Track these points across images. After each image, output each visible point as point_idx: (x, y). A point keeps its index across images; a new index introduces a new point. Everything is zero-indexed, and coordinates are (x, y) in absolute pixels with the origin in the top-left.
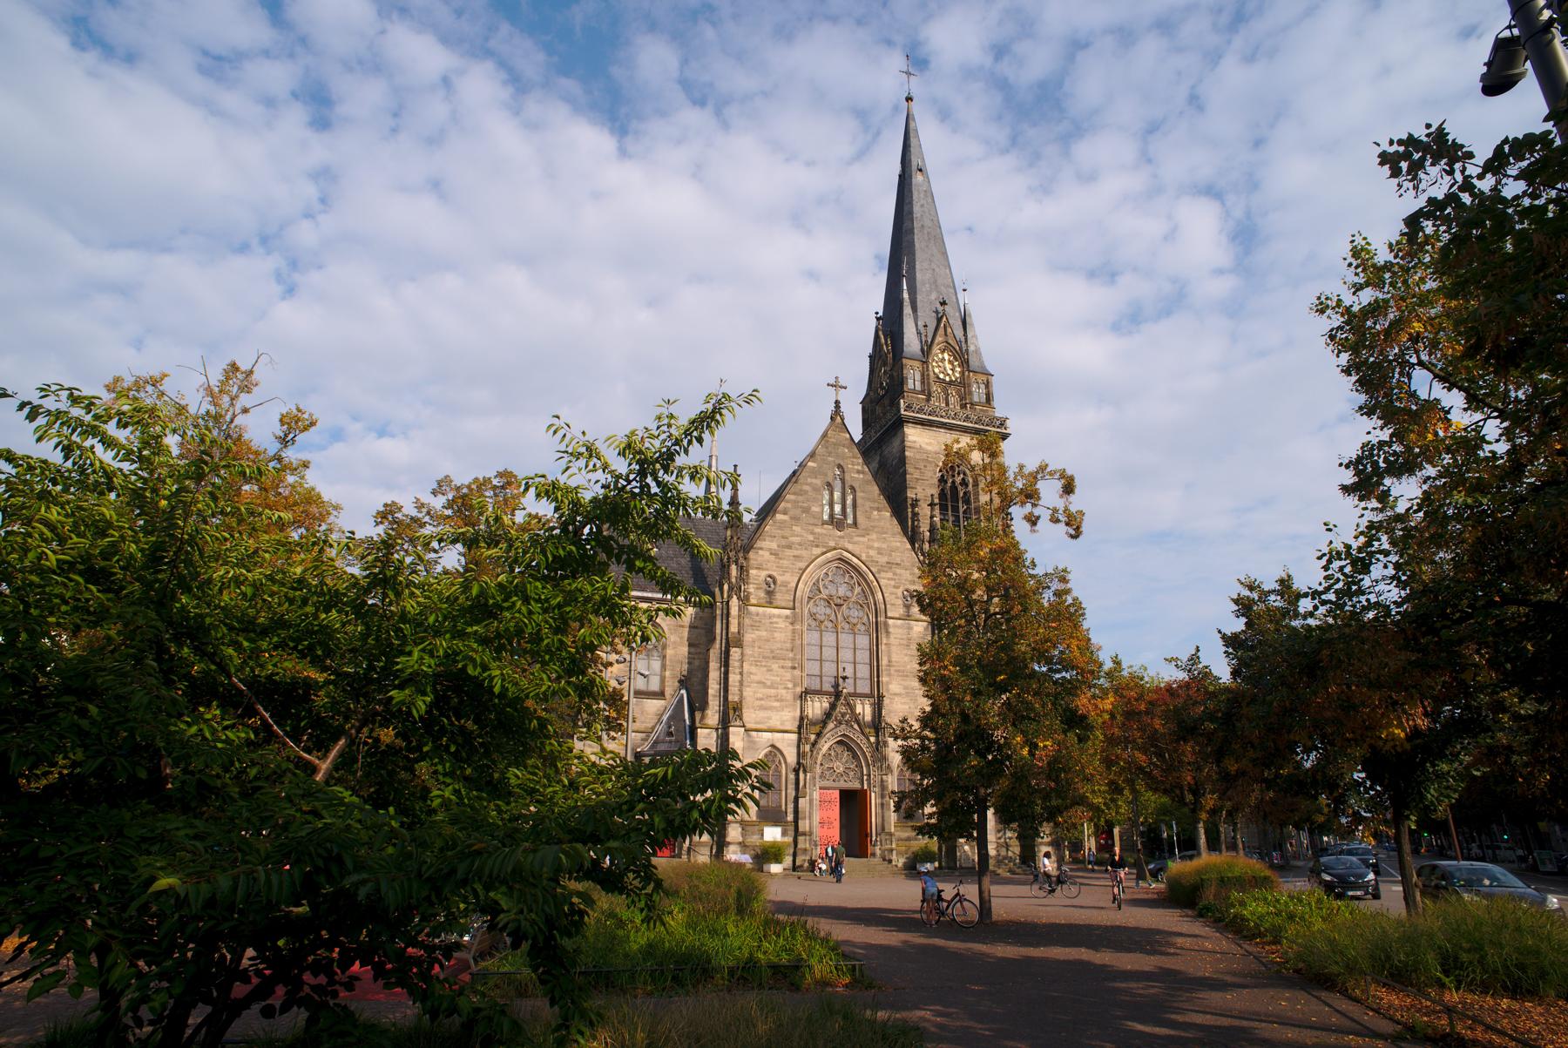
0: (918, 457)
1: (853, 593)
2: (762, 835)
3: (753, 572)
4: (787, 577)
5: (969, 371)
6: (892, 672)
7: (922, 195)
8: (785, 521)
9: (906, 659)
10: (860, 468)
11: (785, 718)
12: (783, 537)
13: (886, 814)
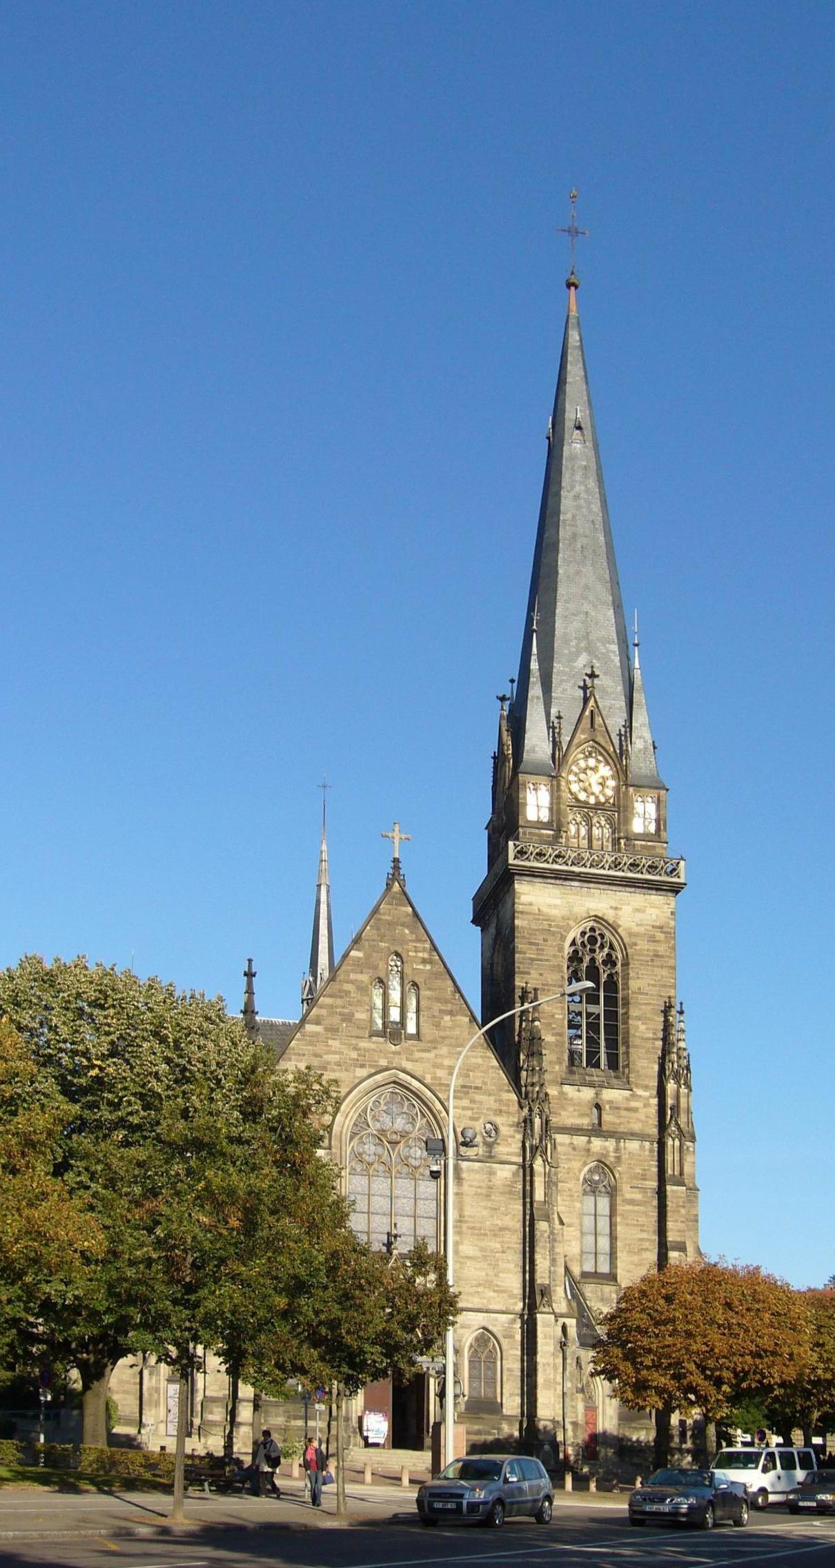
0: (533, 927)
1: (414, 1126)
5: (627, 785)
6: (464, 1229)
7: (578, 477)
8: (317, 1034)
9: (485, 1213)
10: (426, 955)
12: (316, 1055)
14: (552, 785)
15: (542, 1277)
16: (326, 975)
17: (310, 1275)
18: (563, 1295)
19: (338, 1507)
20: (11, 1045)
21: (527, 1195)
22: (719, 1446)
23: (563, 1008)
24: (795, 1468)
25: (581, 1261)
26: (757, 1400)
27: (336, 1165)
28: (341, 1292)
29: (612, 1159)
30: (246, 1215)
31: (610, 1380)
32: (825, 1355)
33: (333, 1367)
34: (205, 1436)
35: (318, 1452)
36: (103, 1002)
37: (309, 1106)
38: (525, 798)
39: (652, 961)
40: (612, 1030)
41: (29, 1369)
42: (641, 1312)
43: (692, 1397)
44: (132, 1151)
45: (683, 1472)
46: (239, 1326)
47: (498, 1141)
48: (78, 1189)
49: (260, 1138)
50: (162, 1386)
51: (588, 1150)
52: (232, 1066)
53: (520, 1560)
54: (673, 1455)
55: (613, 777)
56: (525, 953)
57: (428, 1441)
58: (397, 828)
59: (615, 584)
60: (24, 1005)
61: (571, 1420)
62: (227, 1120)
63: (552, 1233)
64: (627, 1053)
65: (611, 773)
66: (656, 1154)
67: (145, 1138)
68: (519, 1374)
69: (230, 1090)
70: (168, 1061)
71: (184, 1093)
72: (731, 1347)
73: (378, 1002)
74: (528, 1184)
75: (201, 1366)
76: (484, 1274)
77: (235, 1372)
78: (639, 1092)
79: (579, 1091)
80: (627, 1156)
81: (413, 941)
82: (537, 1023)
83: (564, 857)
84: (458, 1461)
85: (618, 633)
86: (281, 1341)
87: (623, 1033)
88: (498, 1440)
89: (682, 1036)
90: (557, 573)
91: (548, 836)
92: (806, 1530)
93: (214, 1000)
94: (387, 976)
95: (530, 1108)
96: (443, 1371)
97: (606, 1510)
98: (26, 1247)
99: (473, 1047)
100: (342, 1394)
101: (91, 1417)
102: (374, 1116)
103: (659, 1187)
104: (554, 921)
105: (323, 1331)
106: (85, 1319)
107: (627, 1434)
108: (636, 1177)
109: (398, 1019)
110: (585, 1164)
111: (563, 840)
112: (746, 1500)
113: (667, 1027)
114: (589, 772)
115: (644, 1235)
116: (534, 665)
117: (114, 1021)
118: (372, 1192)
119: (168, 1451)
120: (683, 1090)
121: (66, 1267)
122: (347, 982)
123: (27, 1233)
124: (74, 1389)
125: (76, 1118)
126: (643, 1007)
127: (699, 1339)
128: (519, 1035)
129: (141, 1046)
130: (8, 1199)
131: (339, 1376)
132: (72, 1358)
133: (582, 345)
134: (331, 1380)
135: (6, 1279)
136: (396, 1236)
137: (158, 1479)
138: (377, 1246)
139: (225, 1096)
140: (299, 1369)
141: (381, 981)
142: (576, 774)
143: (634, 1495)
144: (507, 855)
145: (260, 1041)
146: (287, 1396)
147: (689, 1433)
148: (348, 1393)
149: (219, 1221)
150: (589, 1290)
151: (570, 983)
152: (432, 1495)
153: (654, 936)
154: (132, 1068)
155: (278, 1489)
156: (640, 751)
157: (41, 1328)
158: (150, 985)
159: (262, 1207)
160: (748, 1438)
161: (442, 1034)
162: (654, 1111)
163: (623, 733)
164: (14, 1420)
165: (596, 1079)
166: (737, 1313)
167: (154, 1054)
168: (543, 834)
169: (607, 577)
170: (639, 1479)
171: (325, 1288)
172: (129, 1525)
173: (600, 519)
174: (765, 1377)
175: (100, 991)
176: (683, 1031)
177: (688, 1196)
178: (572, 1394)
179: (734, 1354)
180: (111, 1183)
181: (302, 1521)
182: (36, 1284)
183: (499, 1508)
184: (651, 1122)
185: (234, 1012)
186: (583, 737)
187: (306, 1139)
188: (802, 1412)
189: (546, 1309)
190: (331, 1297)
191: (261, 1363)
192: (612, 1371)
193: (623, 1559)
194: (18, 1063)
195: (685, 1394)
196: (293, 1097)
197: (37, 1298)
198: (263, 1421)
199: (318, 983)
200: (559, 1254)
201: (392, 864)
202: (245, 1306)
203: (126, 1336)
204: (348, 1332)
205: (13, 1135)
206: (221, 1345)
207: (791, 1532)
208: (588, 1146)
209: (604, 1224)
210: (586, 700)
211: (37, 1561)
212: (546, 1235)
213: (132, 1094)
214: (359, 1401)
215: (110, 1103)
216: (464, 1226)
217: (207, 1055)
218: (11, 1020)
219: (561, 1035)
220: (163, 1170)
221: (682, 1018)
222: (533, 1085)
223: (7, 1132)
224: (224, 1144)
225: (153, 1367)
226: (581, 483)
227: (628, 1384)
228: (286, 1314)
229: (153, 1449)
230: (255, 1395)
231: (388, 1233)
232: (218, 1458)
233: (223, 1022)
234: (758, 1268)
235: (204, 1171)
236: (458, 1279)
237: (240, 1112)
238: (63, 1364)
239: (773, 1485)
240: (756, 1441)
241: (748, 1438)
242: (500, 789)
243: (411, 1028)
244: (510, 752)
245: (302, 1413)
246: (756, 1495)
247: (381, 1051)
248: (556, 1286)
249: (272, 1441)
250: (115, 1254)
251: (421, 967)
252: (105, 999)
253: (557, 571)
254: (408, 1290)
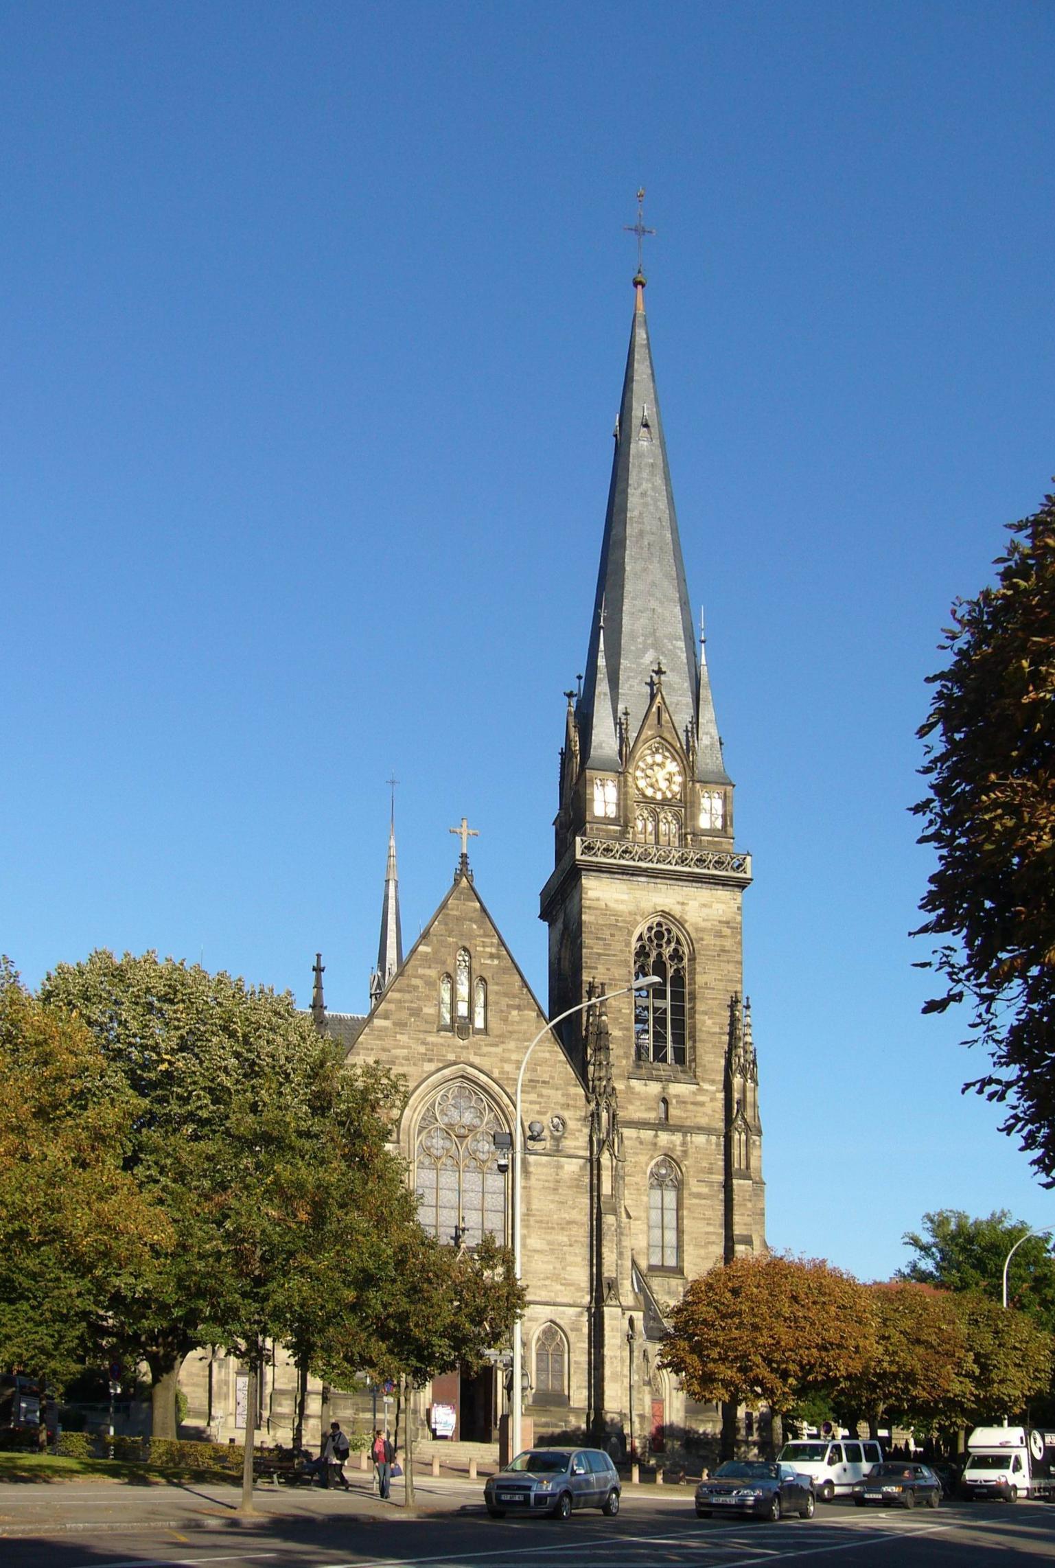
1: (482, 1120)
5: (694, 781)
6: (532, 1223)
7: (645, 475)
8: (386, 1028)
9: (552, 1206)
10: (494, 950)
12: (384, 1050)
14: (619, 781)
15: (609, 1271)
16: (395, 969)
17: (378, 1268)
18: (630, 1288)
19: (406, 1500)
20: (81, 1040)
21: (595, 1189)
22: (785, 1438)
23: (630, 1003)
24: (861, 1461)
25: (648, 1255)
26: (823, 1392)
27: (405, 1158)
28: (409, 1285)
29: (679, 1153)
30: (314, 1209)
31: (677, 1372)
32: (891, 1348)
33: (401, 1360)
34: (274, 1429)
35: (386, 1444)
36: (172, 997)
37: (377, 1100)
38: (592, 794)
39: (719, 956)
40: (679, 1025)
41: (99, 1362)
42: (708, 1305)
43: (759, 1390)
44: (202, 1146)
45: (749, 1464)
46: (308, 1320)
48: (148, 1182)
49: (329, 1132)
50: (231, 1378)
51: (655, 1144)
52: (301, 1060)
53: (587, 1552)
54: (739, 1448)
55: (680, 773)
56: (592, 948)
57: (496, 1434)
58: (465, 824)
59: (681, 580)
60: (94, 1000)
61: (638, 1413)
62: (296, 1114)
63: (619, 1226)
64: (694, 1048)
65: (677, 769)
66: (722, 1148)
67: (214, 1132)
68: (587, 1366)
69: (299, 1085)
70: (237, 1055)
71: (253, 1087)
72: (797, 1340)
73: (446, 997)
74: (595, 1178)
75: (270, 1359)
76: (551, 1267)
77: (303, 1365)
78: (706, 1086)
79: (646, 1085)
81: (480, 936)
82: (604, 1018)
83: (631, 853)
84: (525, 1453)
85: (685, 629)
86: (350, 1334)
87: (690, 1028)
88: (565, 1433)
89: (749, 1031)
90: (624, 570)
91: (615, 832)
92: (872, 1522)
93: (283, 994)
94: (455, 971)
95: (597, 1102)
96: (510, 1365)
97: (672, 1502)
98: (96, 1241)
99: (541, 1041)
100: (410, 1387)
101: (161, 1410)
102: (442, 1110)
103: (726, 1180)
104: (621, 916)
105: (392, 1324)
106: (155, 1312)
107: (694, 1426)
108: (702, 1171)
109: (466, 1014)
110: (652, 1158)
111: (630, 836)
112: (812, 1493)
113: (734, 1021)
114: (655, 768)
115: (711, 1229)
116: (601, 662)
117: (184, 1015)
118: (440, 1186)
119: (237, 1443)
120: (750, 1084)
121: (135, 1260)
122: (415, 977)
123: (96, 1226)
124: (144, 1382)
125: (146, 1112)
127: (765, 1332)
128: (587, 1029)
129: (210, 1041)
130: (78, 1193)
131: (408, 1369)
132: (142, 1351)
133: (648, 344)
134: (399, 1373)
135: (76, 1272)
136: (464, 1230)
137: (227, 1472)
138: (445, 1240)
139: (294, 1090)
140: (368, 1362)
141: (449, 976)
142: (643, 770)
143: (701, 1487)
144: (574, 851)
145: (329, 1035)
146: (355, 1389)
147: (755, 1426)
148: (416, 1386)
149: (288, 1215)
150: (656, 1283)
151: (637, 978)
152: (500, 1487)
153: (721, 931)
154: (201, 1062)
155: (347, 1481)
156: (707, 747)
157: (111, 1321)
158: (219, 980)
159: (330, 1201)
160: (814, 1431)
161: (510, 1028)
163: (689, 729)
164: (84, 1413)
165: (662, 1073)
166: (803, 1306)
167: (223, 1048)
168: (610, 830)
169: (674, 574)
170: (706, 1471)
171: (394, 1281)
172: (199, 1516)
173: (666, 516)
174: (831, 1370)
175: (170, 986)
176: (749, 1025)
177: (754, 1190)
178: (639, 1387)
179: (800, 1347)
180: (180, 1177)
181: (371, 1512)
182: (106, 1278)
183: (567, 1500)
184: (717, 1116)
185: (303, 1006)
186: (650, 733)
187: (375, 1133)
188: (868, 1404)
189: (613, 1303)
190: (399, 1290)
191: (330, 1356)
192: (680, 1363)
193: (690, 1551)
194: (88, 1057)
195: (752, 1387)
196: (362, 1092)
197: (107, 1291)
198: (331, 1414)
199: (387, 978)
201: (460, 860)
202: (314, 1299)
203: (195, 1329)
204: (416, 1325)
205: (83, 1129)
206: (290, 1338)
207: (856, 1523)
208: (655, 1140)
209: (670, 1218)
210: (653, 697)
211: (107, 1553)
212: (613, 1228)
213: (201, 1088)
214: (427, 1394)
215: (179, 1097)
216: (532, 1219)
217: (276, 1049)
218: (81, 1015)
219: (627, 1029)
220: (232, 1163)
221: (748, 1013)
222: (600, 1079)
223: (77, 1126)
224: (293, 1138)
225: (222, 1360)
226: (648, 480)
227: (695, 1376)
228: (354, 1308)
229: (222, 1442)
230: (324, 1388)
231: (456, 1227)
232: (286, 1450)
233: (292, 1017)
234: (824, 1261)
235: (273, 1165)
236: (525, 1273)
237: (309, 1106)
238: (132, 1357)
239: (839, 1477)
240: (822, 1433)
241: (814, 1431)
242: (567, 785)
243: (479, 1023)
244: (577, 748)
245: (371, 1405)
246: (822, 1487)
248: (623, 1279)
249: (341, 1433)
250: (185, 1248)
251: (488, 962)
252: (175, 994)
253: (624, 568)
254: (476, 1283)
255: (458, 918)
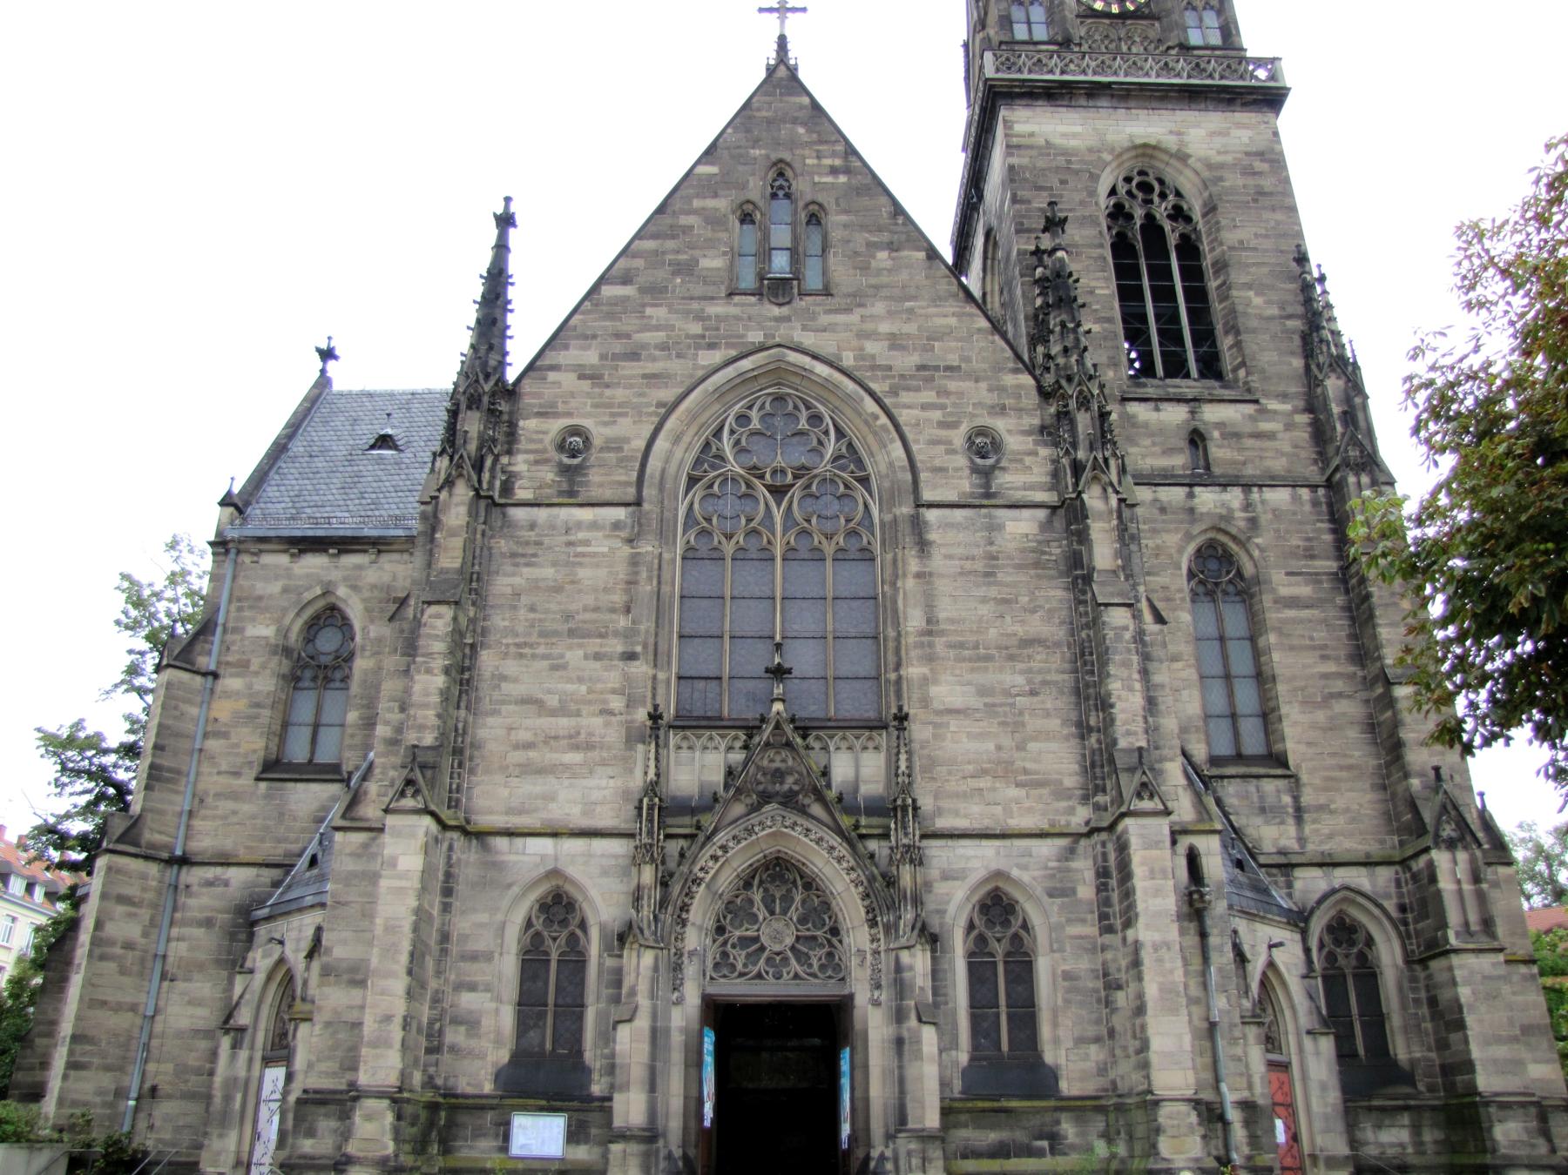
0: (1041, 163)
2: (506, 1137)
3: (527, 425)
4: (624, 427)
8: (625, 300)
9: (985, 610)
10: (838, 162)
11: (596, 795)
12: (618, 336)
13: (911, 1071)
29: (1242, 524)
39: (1255, 201)
47: (1002, 464)
51: (1191, 510)
64: (1238, 345)
76: (991, 746)
78: (1273, 405)
79: (1157, 409)
80: (1270, 516)
102: (738, 442)
108: (1293, 554)
115: (1331, 667)
126: (1253, 270)
161: (873, 281)
162: (1306, 436)
200: (1163, 686)
208: (1189, 504)
216: (939, 642)
243: (813, 280)
247: (750, 318)
255: (769, 122)
